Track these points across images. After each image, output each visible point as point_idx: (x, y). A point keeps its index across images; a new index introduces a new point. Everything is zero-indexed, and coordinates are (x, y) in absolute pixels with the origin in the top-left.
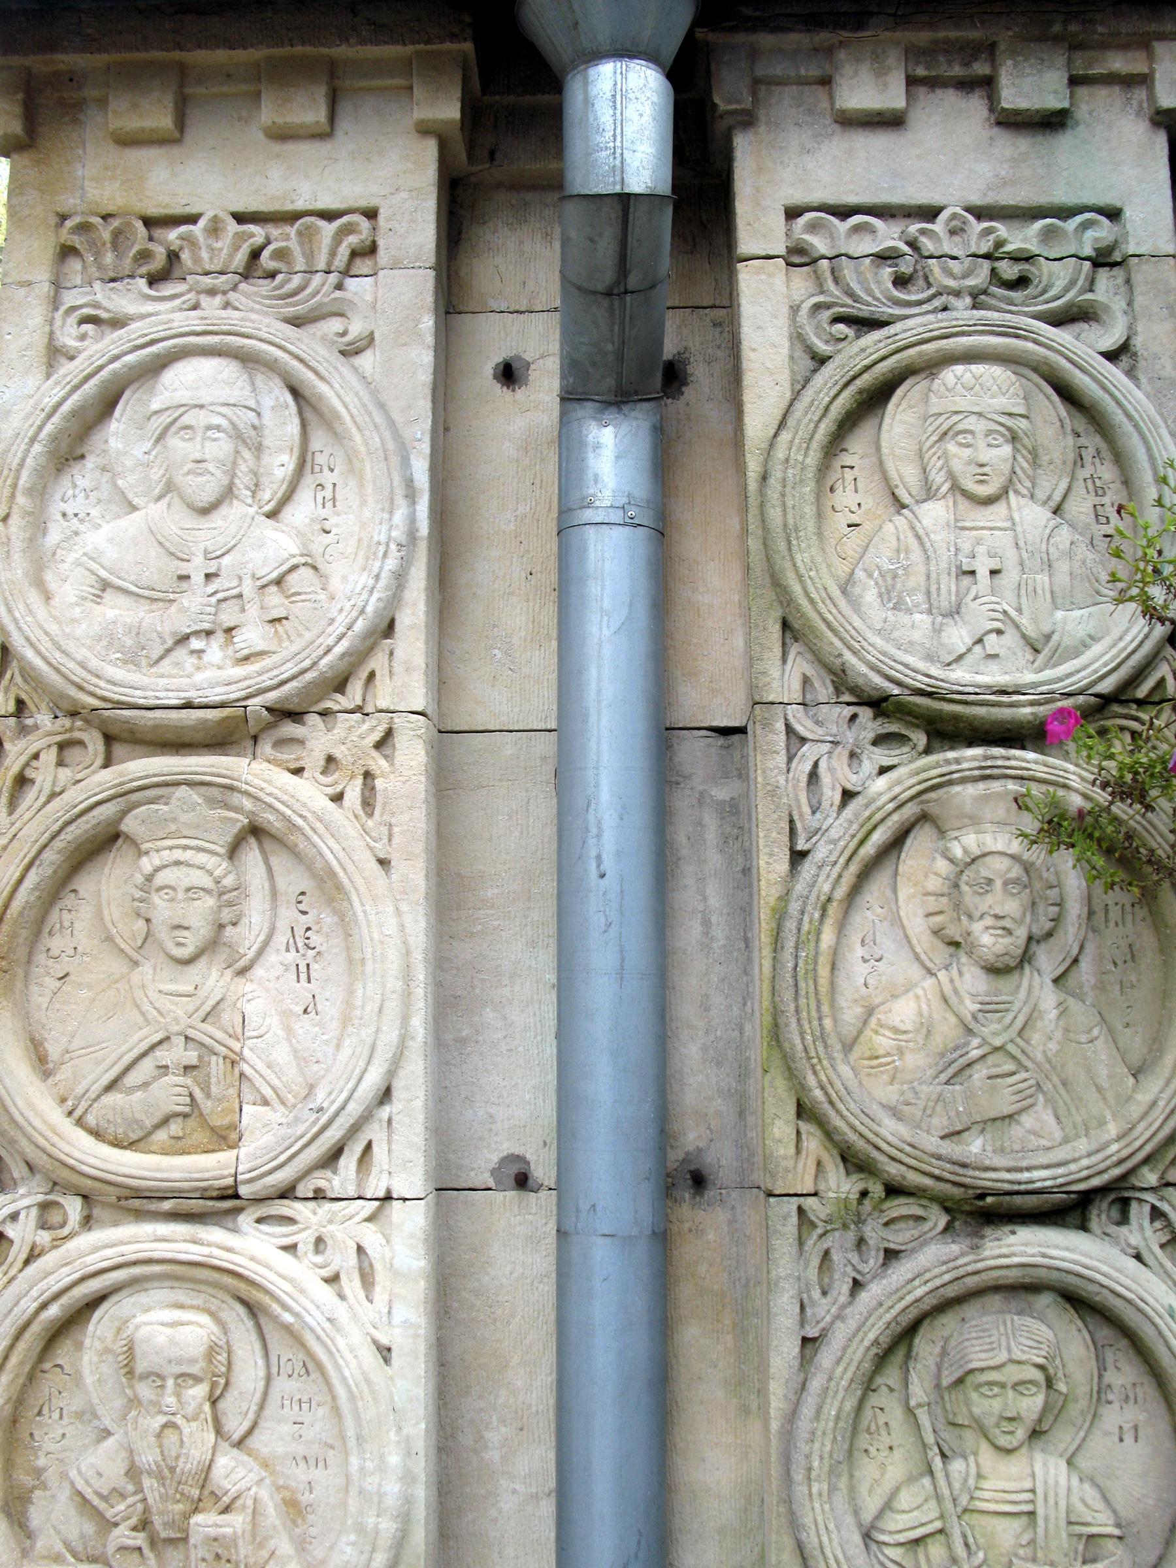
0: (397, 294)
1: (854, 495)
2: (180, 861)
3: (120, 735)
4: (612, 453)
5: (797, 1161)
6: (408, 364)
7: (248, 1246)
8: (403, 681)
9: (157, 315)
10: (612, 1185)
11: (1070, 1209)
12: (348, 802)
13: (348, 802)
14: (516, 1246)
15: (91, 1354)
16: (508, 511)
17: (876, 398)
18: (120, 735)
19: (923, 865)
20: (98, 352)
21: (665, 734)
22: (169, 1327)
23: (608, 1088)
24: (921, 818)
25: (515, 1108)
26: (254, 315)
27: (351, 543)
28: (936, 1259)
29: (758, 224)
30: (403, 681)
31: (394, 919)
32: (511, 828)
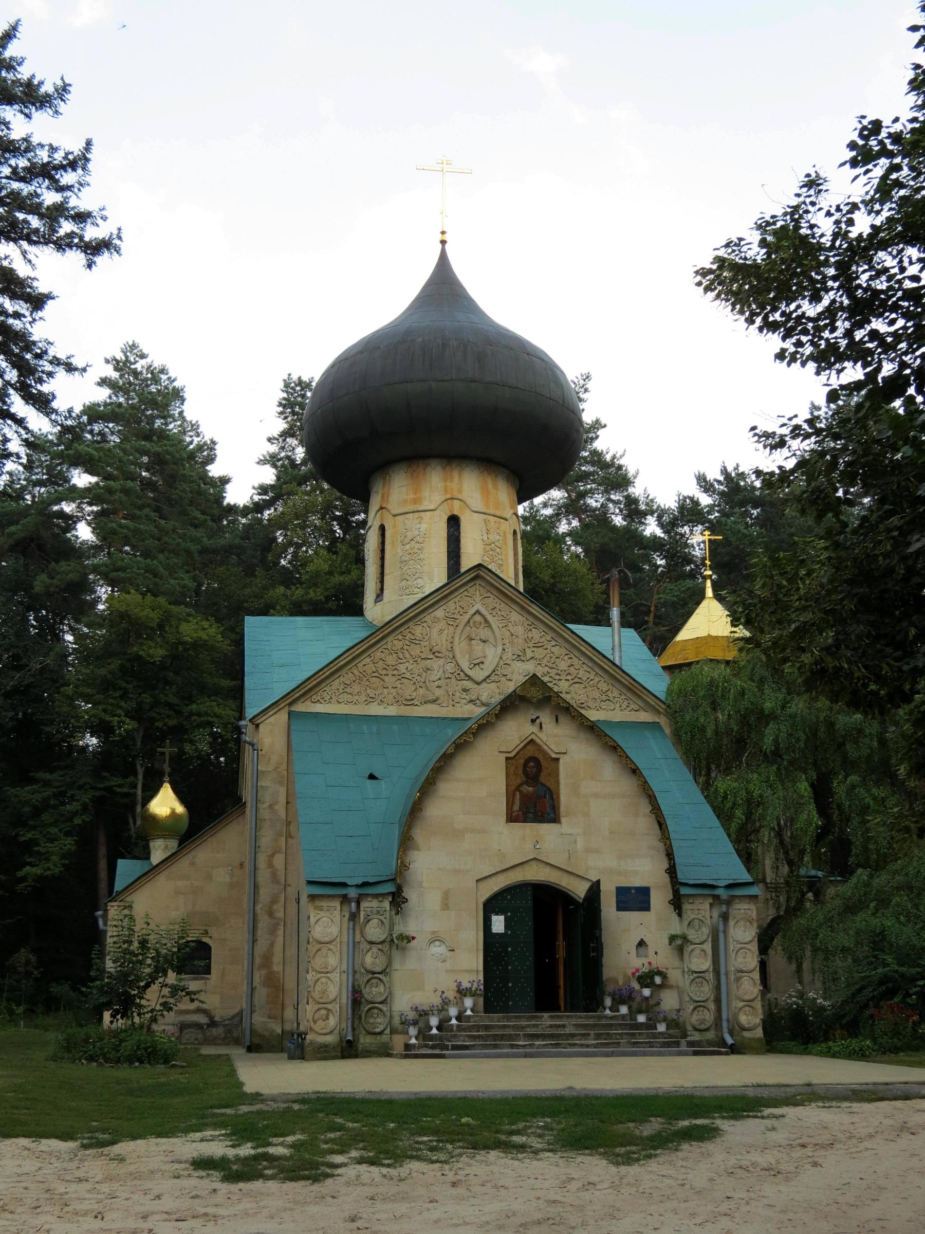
0: (337, 913)
1: (367, 928)
2: (324, 951)
3: (320, 943)
5: (363, 970)
6: (338, 918)
7: (329, 975)
8: (338, 940)
9: (322, 914)
11: (379, 973)
14: (344, 976)
15: (319, 983)
19: (370, 952)
20: (319, 916)
21: (354, 942)
22: (324, 980)
23: (351, 965)
24: (370, 949)
25: (344, 968)
26: (328, 914)
27: (334, 930)
28: (371, 976)
29: (362, 908)
30: (338, 940)
31: (338, 955)
32: (345, 949)
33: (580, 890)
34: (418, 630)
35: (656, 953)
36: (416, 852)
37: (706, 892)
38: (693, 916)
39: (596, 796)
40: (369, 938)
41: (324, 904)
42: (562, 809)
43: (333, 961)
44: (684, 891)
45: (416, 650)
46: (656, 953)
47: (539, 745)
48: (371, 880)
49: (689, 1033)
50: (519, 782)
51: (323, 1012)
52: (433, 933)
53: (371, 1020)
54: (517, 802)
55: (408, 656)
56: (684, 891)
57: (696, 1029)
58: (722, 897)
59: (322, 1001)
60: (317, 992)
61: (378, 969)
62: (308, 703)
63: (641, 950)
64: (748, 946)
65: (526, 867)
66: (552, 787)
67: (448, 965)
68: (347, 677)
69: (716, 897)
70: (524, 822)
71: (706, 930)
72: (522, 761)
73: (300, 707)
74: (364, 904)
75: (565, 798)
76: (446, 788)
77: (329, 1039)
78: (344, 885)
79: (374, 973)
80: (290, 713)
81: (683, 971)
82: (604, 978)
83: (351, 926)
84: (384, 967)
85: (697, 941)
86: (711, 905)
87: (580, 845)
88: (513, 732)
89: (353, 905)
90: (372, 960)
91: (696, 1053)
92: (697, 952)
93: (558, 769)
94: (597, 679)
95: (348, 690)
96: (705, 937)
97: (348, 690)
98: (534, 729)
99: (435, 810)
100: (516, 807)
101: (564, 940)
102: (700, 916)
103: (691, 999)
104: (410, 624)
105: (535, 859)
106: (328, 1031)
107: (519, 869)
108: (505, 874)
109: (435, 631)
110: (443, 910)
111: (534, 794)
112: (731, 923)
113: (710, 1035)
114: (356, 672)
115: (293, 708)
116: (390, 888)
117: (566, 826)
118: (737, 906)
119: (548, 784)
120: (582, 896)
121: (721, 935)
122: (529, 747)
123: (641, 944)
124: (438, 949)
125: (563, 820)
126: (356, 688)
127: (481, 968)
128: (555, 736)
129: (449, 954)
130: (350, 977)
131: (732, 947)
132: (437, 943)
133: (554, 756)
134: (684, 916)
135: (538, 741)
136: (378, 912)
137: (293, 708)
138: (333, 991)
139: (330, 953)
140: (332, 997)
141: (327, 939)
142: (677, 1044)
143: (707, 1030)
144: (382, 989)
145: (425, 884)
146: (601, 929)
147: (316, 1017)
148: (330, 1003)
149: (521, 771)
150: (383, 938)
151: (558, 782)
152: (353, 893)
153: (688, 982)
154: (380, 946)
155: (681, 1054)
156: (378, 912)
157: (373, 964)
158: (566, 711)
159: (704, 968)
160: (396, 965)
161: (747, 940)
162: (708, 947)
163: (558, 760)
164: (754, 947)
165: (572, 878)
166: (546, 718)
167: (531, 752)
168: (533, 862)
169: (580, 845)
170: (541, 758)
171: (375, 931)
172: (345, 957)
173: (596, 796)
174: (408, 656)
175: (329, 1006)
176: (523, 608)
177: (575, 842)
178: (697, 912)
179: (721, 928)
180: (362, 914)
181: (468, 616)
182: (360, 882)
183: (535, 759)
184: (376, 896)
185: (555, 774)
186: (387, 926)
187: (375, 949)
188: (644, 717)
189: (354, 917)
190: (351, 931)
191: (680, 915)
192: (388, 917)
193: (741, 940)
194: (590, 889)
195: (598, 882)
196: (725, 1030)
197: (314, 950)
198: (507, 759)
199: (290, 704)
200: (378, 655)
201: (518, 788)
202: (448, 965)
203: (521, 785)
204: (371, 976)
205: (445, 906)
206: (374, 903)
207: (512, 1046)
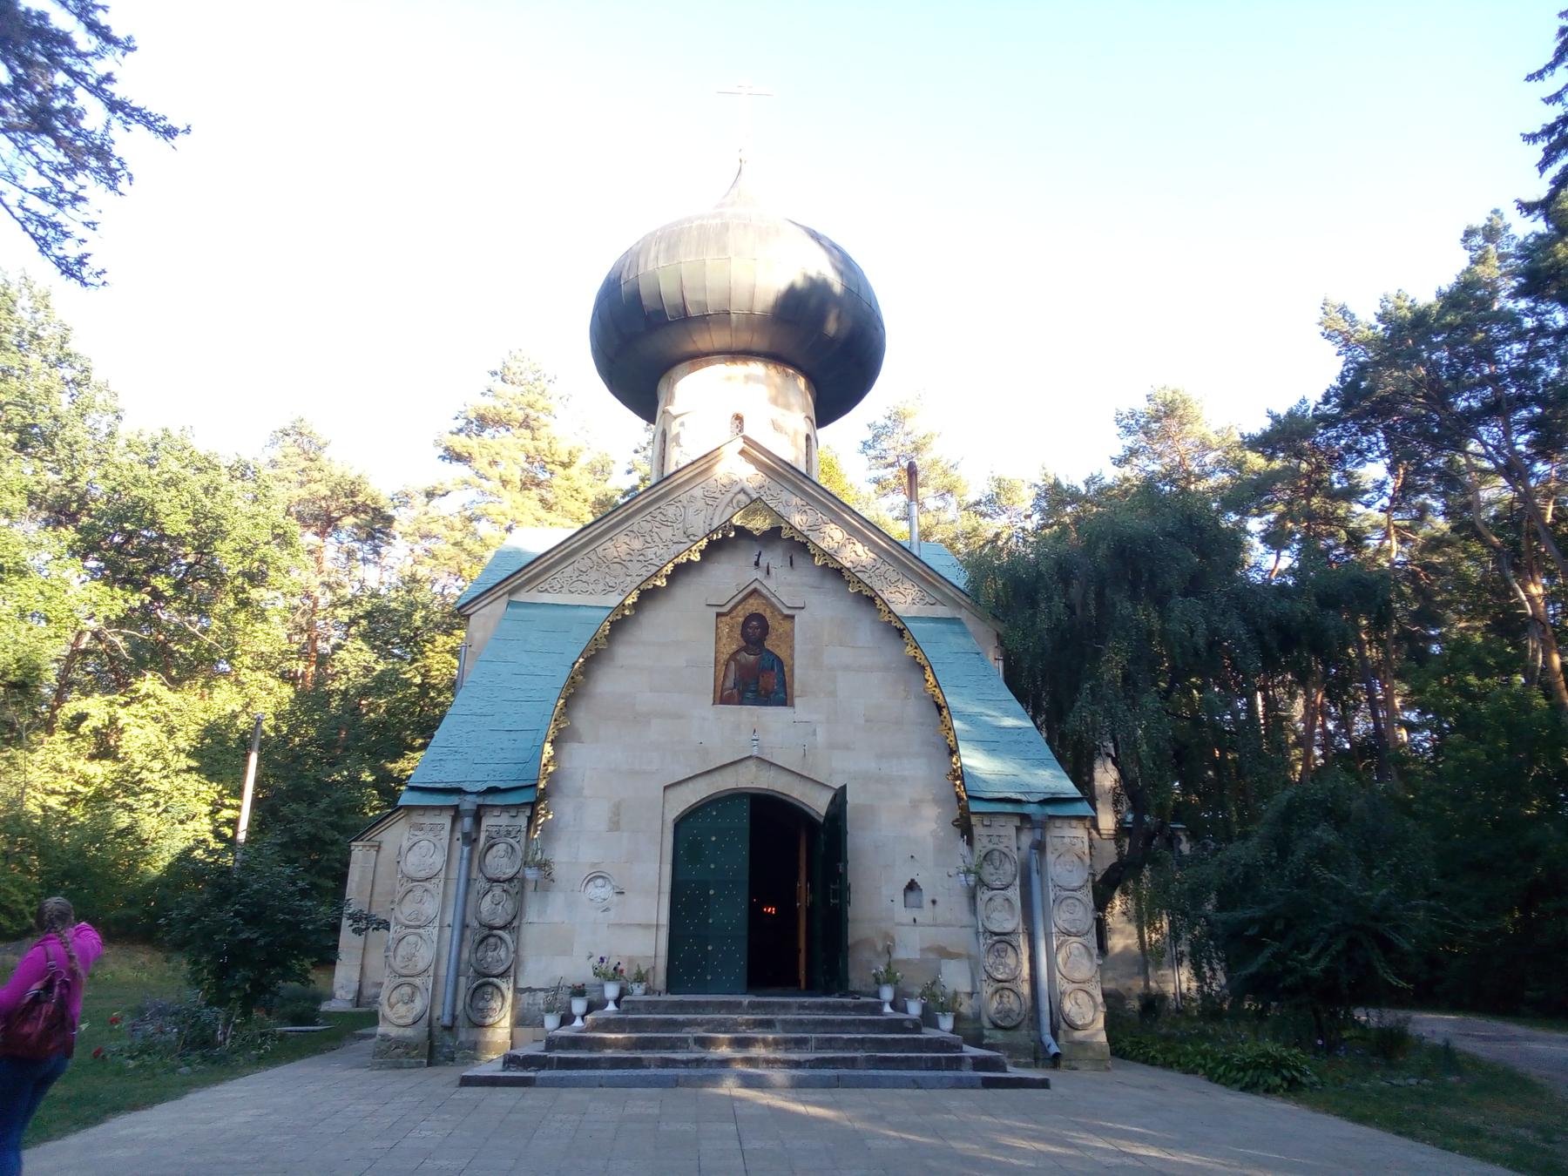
1: (489, 857)
2: (418, 893)
3: (413, 880)
4: (466, 849)
7: (421, 931)
10: (457, 926)
12: (436, 887)
13: (436, 887)
14: (448, 931)
16: (456, 855)
17: (492, 846)
18: (413, 880)
20: (416, 839)
25: (449, 919)
26: (430, 836)
27: (438, 860)
29: (483, 827)
30: (442, 875)
33: (819, 803)
34: (671, 511)
35: (934, 902)
36: (576, 745)
37: (1009, 808)
38: (991, 846)
39: (846, 668)
40: (491, 873)
41: (427, 820)
42: (797, 686)
43: (430, 907)
44: (975, 807)
45: (667, 533)
46: (934, 902)
47: (765, 597)
48: (502, 786)
49: (986, 1033)
50: (734, 647)
51: (406, 990)
52: (594, 865)
53: (481, 1005)
54: (732, 676)
55: (656, 539)
56: (975, 807)
57: (997, 1027)
58: (1037, 817)
59: (405, 972)
60: (399, 958)
61: (499, 922)
62: (534, 592)
63: (912, 896)
64: (1078, 894)
65: (741, 768)
66: (781, 653)
67: (611, 916)
68: (581, 562)
69: (1025, 818)
70: (741, 703)
71: (1009, 868)
72: (741, 619)
73: (522, 597)
74: (488, 822)
75: (802, 673)
76: (627, 653)
77: (409, 1032)
78: (458, 791)
79: (492, 928)
80: (510, 604)
81: (977, 933)
82: (850, 941)
83: (465, 854)
84: (509, 918)
85: (998, 884)
86: (1018, 829)
87: (821, 737)
88: (729, 578)
89: (467, 823)
90: (492, 907)
91: (989, 1084)
92: (999, 901)
93: (793, 630)
94: (883, 569)
95: (584, 578)
96: (1008, 880)
97: (584, 578)
98: (759, 574)
99: (608, 684)
100: (730, 683)
101: (809, 879)
102: (1001, 847)
103: (990, 976)
104: (661, 503)
105: (750, 757)
106: (410, 1021)
107: (731, 770)
108: (708, 779)
109: (690, 511)
110: (610, 830)
111: (756, 670)
112: (1050, 857)
113: (1022, 1037)
114: (594, 558)
115: (515, 598)
116: (528, 796)
117: (802, 710)
118: (1057, 832)
119: (777, 652)
120: (823, 813)
121: (1035, 876)
122: (751, 601)
123: (912, 886)
124: (599, 891)
125: (797, 701)
126: (593, 575)
127: (664, 918)
128: (785, 584)
129: (616, 898)
130: (456, 933)
131: (1052, 896)
132: (600, 882)
133: (786, 612)
134: (978, 846)
135: (764, 591)
136: (509, 833)
137: (515, 598)
138: (425, 956)
139: (427, 897)
140: (421, 966)
141: (423, 874)
142: (956, 1063)
143: (1015, 1028)
144: (502, 953)
145: (586, 792)
146: (846, 862)
147: (393, 1000)
148: (418, 975)
149: (738, 631)
150: (510, 872)
151: (792, 648)
152: (468, 803)
153: (983, 949)
154: (506, 886)
155: (959, 1084)
156: (509, 833)
157: (494, 912)
158: (800, 548)
159: (1009, 927)
160: (531, 914)
161: (1076, 884)
162: (1014, 894)
163: (792, 617)
164: (1087, 896)
165: (809, 785)
166: (774, 558)
167: (753, 606)
168: (749, 763)
169: (821, 737)
170: (768, 615)
171: (500, 862)
172: (451, 902)
173: (846, 668)
174: (656, 539)
175: (417, 981)
176: (797, 487)
177: (814, 733)
178: (995, 840)
179: (1034, 867)
180: (483, 836)
181: (730, 495)
182: (484, 787)
183: (760, 618)
184: (506, 808)
185: (790, 636)
186: (520, 854)
187: (497, 890)
188: (942, 611)
189: (470, 840)
190: (465, 862)
191: (970, 842)
192: (523, 840)
193: (1065, 884)
194: (832, 802)
195: (844, 788)
196: (1046, 1029)
197: (403, 890)
198: (719, 615)
199: (511, 593)
200: (622, 538)
201: (733, 656)
202: (612, 913)
203: (737, 652)
204: (486, 932)
205: (615, 825)
206: (504, 820)
207: (666, 1063)
